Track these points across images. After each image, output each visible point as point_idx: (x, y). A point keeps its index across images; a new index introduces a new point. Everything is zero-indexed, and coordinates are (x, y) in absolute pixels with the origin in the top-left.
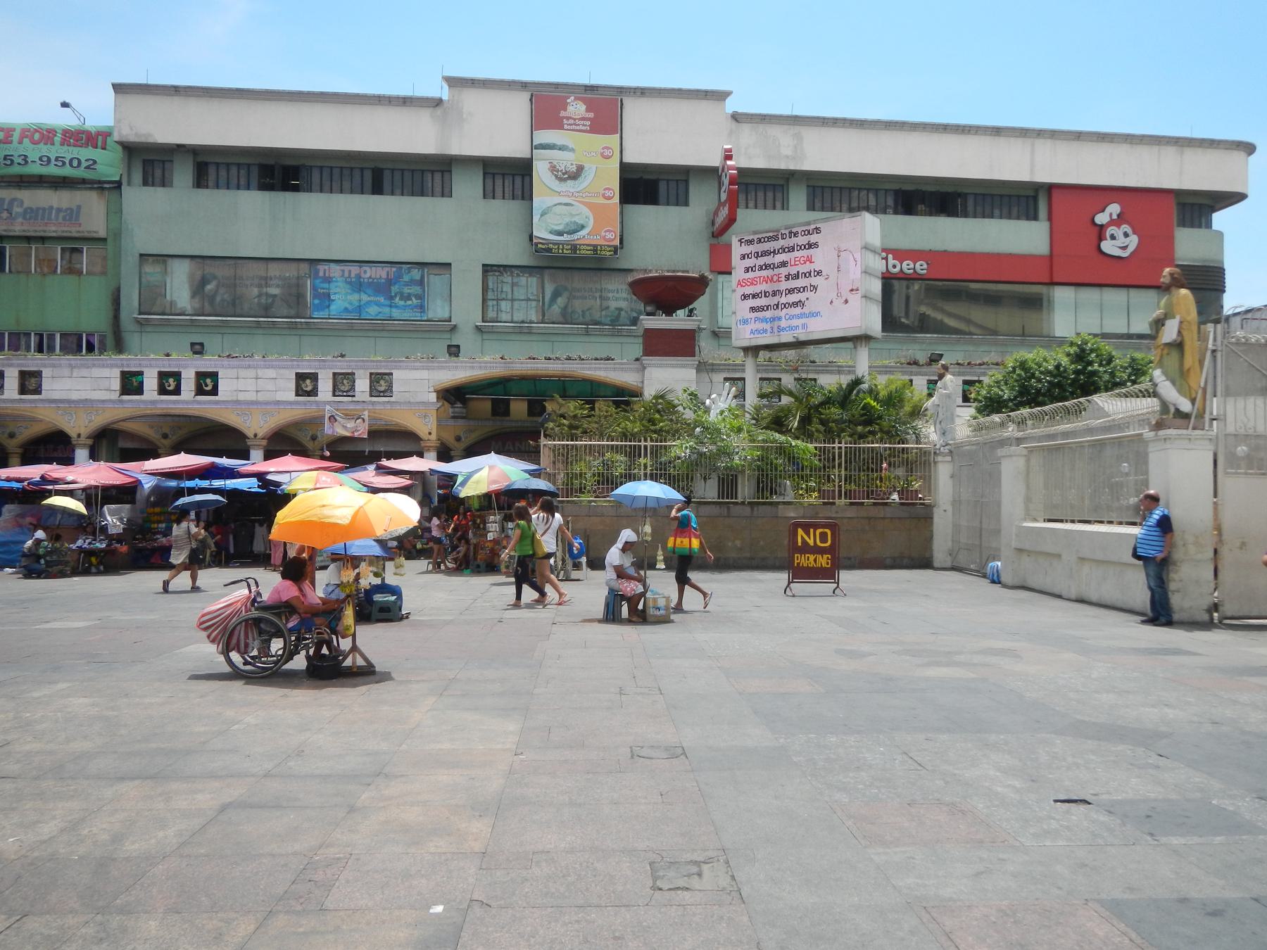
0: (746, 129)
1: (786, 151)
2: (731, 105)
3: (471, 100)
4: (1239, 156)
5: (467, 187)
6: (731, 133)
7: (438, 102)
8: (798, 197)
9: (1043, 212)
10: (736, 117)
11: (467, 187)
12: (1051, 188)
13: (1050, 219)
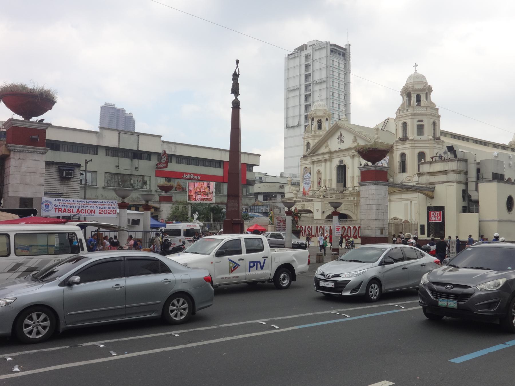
0: (165, 144)
1: (173, 150)
2: (162, 139)
3: (106, 133)
4: (258, 157)
5: (102, 153)
6: (162, 145)
7: (96, 133)
8: (174, 160)
9: (222, 167)
10: (163, 142)
11: (102, 153)
12: (224, 161)
13: (223, 168)
